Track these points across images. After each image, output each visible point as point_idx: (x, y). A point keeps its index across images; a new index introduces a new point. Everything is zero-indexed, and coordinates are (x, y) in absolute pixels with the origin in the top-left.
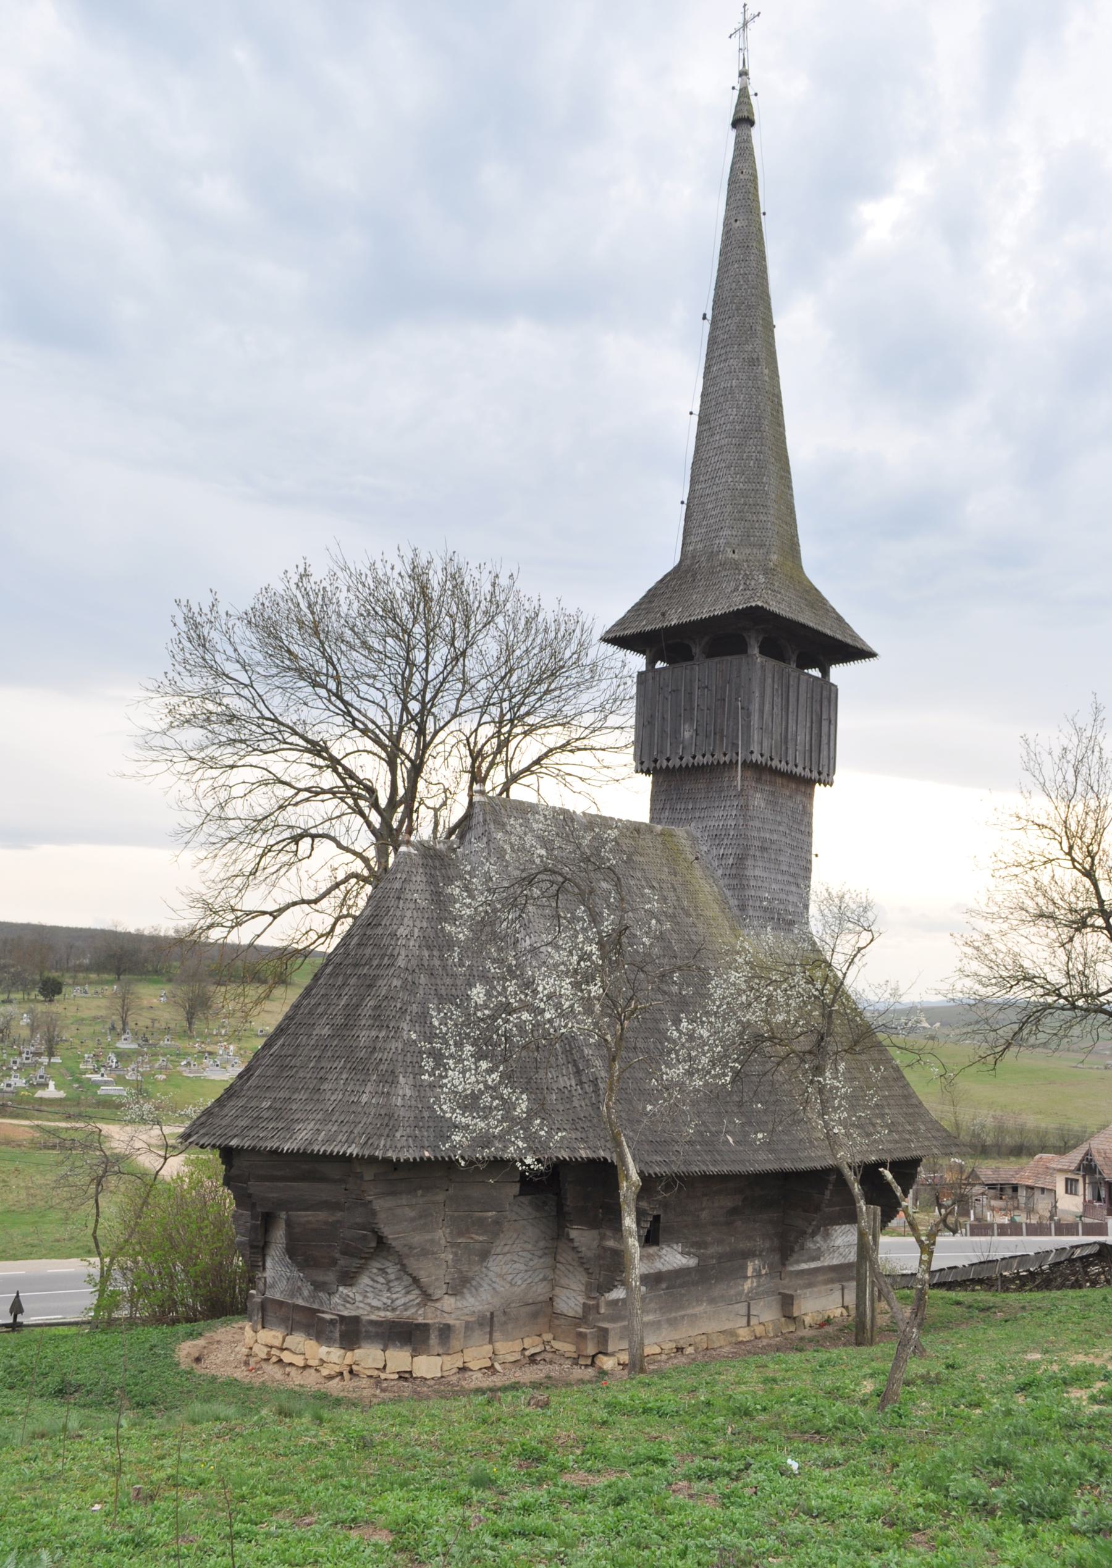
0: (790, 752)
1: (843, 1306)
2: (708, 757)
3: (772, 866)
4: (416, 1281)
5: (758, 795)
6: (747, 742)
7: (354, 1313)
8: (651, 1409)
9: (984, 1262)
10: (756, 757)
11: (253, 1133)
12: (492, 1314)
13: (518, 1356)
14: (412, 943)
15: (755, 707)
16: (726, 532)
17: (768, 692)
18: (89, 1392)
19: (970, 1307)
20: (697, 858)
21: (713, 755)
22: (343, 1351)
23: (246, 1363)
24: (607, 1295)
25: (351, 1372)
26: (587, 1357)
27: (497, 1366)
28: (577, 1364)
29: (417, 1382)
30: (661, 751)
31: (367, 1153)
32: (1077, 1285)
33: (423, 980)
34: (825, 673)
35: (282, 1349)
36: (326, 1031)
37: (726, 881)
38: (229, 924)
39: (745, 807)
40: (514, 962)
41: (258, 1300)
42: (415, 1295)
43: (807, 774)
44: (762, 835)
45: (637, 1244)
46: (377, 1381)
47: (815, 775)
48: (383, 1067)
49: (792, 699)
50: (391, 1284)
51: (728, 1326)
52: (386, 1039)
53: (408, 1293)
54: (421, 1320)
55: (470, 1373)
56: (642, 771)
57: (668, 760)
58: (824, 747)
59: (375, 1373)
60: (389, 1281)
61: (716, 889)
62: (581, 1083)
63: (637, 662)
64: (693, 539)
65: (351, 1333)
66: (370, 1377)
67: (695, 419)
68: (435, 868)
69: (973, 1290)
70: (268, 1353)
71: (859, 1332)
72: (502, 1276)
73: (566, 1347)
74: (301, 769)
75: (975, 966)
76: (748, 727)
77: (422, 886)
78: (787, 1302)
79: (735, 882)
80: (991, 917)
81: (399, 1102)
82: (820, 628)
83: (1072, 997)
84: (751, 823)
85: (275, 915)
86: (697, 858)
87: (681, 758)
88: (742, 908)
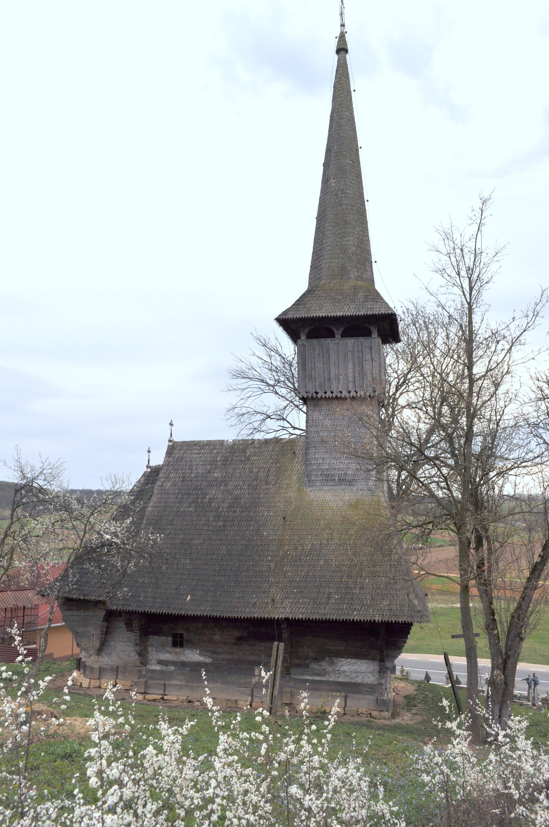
12: (117, 667)
72: (124, 652)
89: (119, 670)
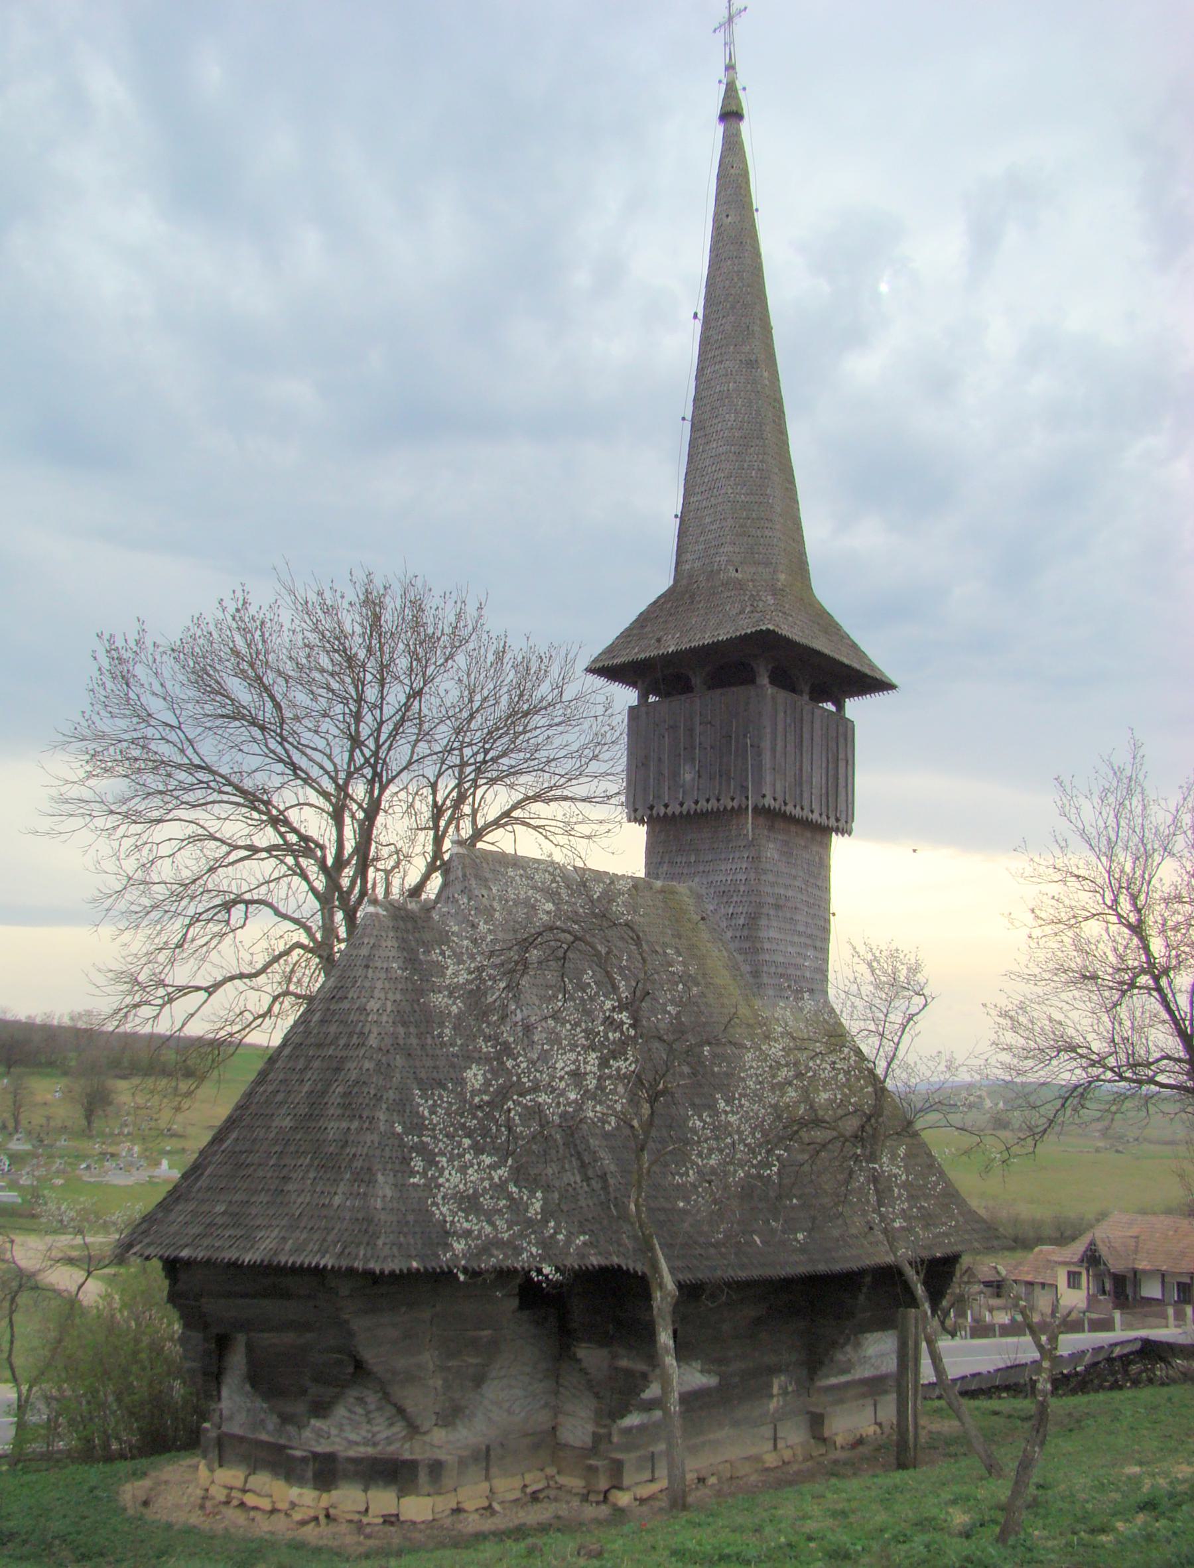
0: (806, 795)
1: (876, 1423)
2: (713, 801)
3: (788, 926)
4: (401, 1411)
5: (771, 845)
6: (759, 783)
7: (328, 1449)
8: (729, 1556)
9: (1011, 1367)
10: (768, 801)
11: (206, 1242)
12: (488, 1448)
13: (517, 1494)
14: (384, 1018)
15: (766, 744)
16: (727, 549)
17: (780, 728)
18: (25, 1542)
19: (1009, 1416)
20: (703, 919)
21: (718, 800)
22: (317, 1493)
23: (202, 1507)
24: (619, 1422)
25: (328, 1516)
26: (598, 1492)
27: (496, 1506)
28: (587, 1500)
29: (406, 1526)
30: (658, 797)
31: (344, 1263)
32: (1116, 1386)
33: (399, 1061)
34: (840, 707)
35: (244, 1491)
36: (287, 1123)
37: (737, 944)
38: (160, 1001)
39: (756, 859)
40: (512, 1039)
41: (213, 1434)
42: (399, 1428)
43: (824, 820)
44: (777, 891)
45: (675, 1364)
46: (359, 1527)
47: (832, 823)
48: (358, 1164)
49: (806, 736)
50: (371, 1416)
51: (753, 1451)
52: (359, 1130)
53: (391, 1425)
54: (407, 1456)
55: (465, 1515)
56: (635, 820)
57: (666, 806)
58: (842, 790)
59: (356, 1517)
60: (368, 1413)
61: (726, 954)
62: (587, 1179)
63: (626, 696)
64: (689, 556)
65: (326, 1471)
66: (351, 1521)
67: (688, 425)
68: (407, 931)
69: (1000, 1398)
70: (228, 1496)
71: (902, 1452)
73: (575, 1483)
74: (236, 825)
75: (1010, 1038)
76: (759, 767)
77: (393, 953)
78: (816, 1422)
79: (747, 945)
80: (1034, 979)
81: (379, 1204)
82: (837, 656)
83: (1119, 1067)
84: (763, 877)
85: (211, 990)
86: (703, 919)
87: (681, 804)
88: (756, 974)
89: (492, 1453)
